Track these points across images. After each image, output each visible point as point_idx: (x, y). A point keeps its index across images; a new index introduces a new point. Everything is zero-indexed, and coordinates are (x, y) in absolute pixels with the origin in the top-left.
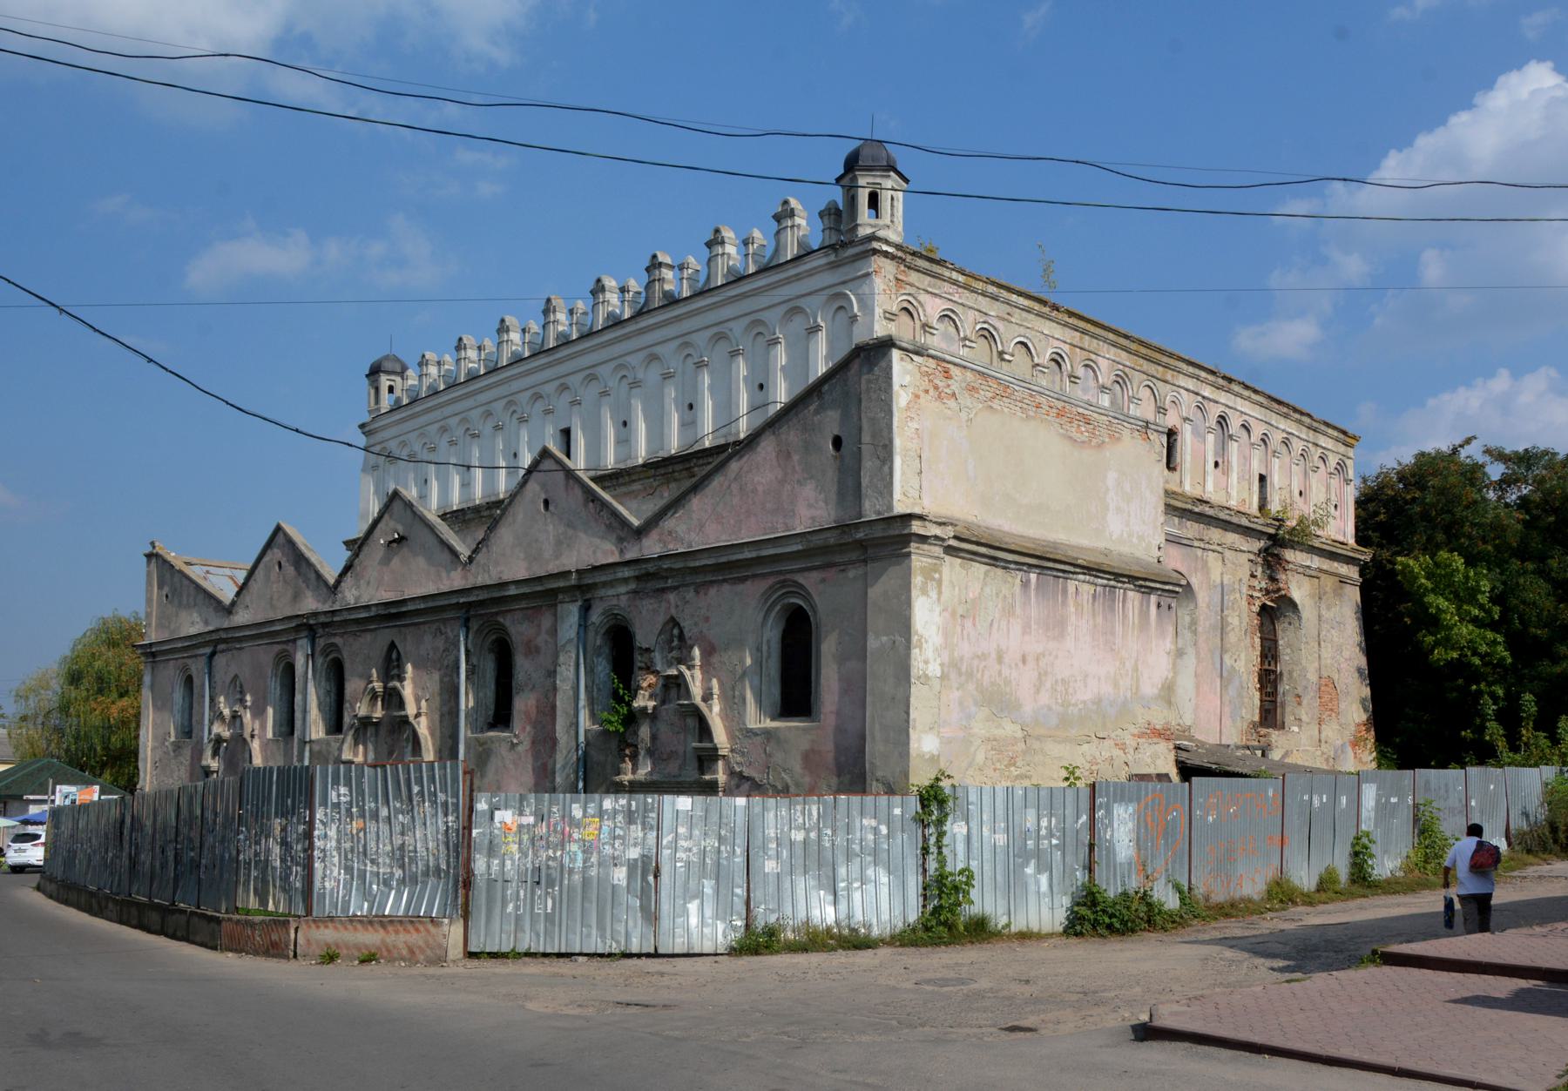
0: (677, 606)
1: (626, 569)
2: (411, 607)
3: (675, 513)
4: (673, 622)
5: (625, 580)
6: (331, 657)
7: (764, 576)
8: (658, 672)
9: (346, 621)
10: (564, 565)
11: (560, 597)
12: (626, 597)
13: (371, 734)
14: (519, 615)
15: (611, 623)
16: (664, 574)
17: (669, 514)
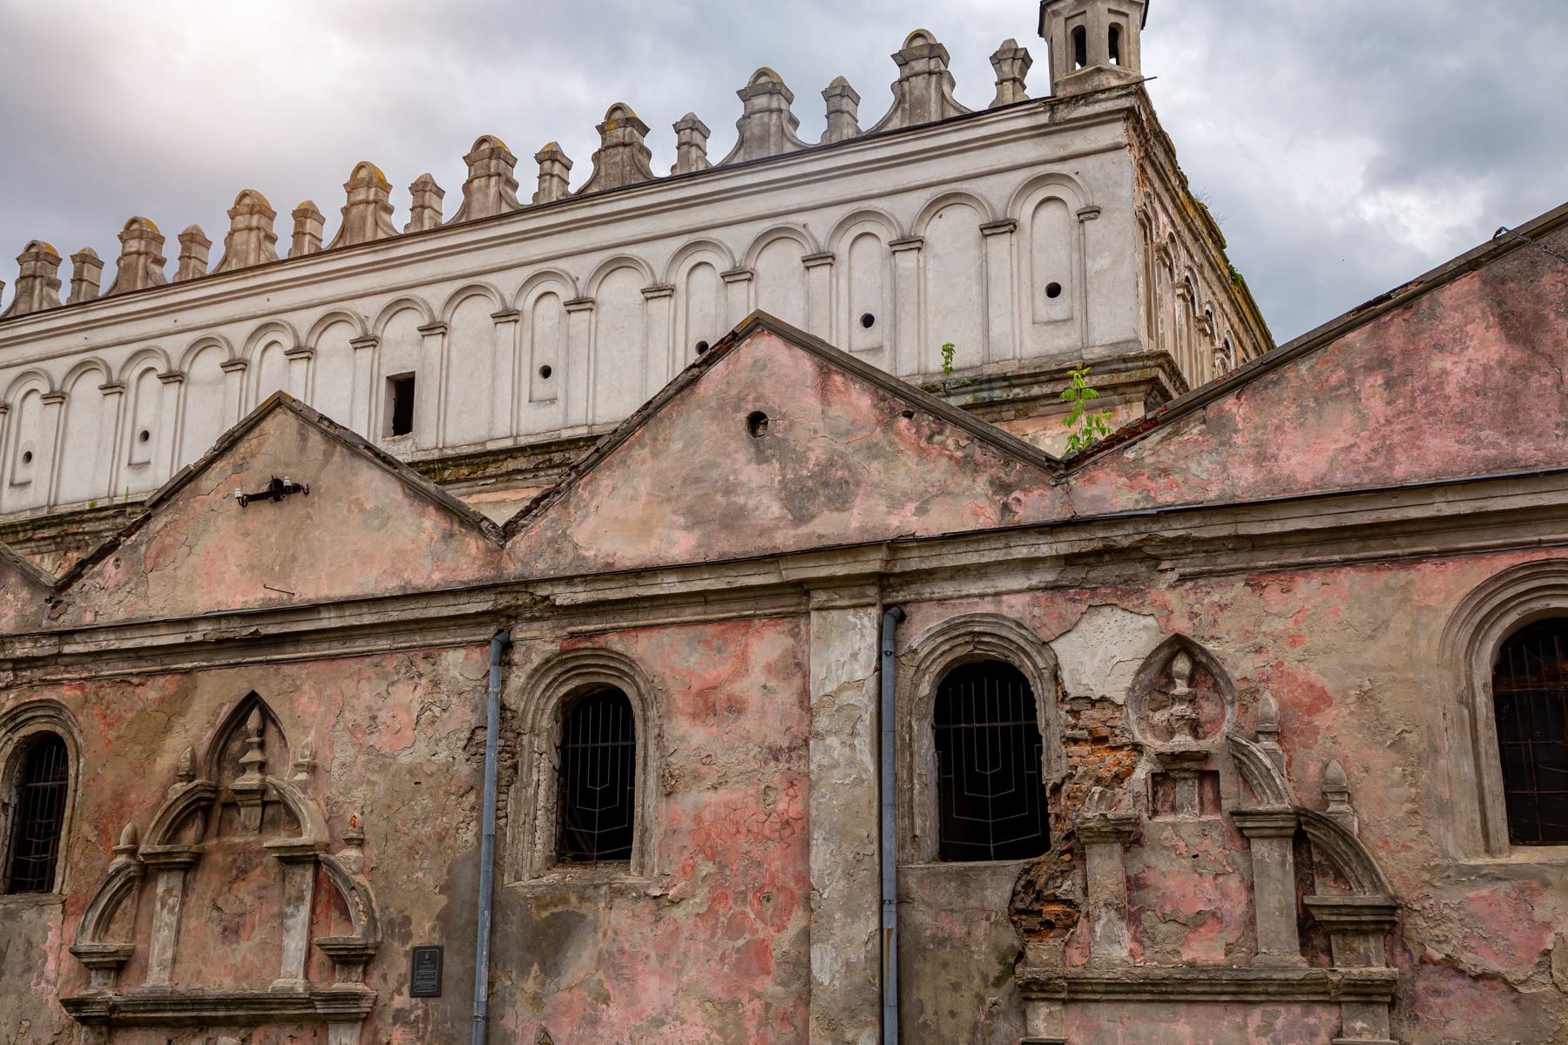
0: (1193, 615)
1: (1049, 539)
2: (329, 620)
3: (1176, 433)
4: (1179, 645)
5: (1029, 564)
6: (23, 732)
7: (1476, 552)
8: (1137, 748)
9: (98, 655)
10: (820, 536)
11: (819, 598)
12: (1026, 598)
13: (169, 891)
14: (667, 636)
15: (960, 652)
16: (1148, 550)
17: (1155, 438)
